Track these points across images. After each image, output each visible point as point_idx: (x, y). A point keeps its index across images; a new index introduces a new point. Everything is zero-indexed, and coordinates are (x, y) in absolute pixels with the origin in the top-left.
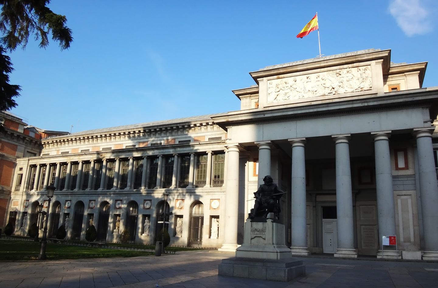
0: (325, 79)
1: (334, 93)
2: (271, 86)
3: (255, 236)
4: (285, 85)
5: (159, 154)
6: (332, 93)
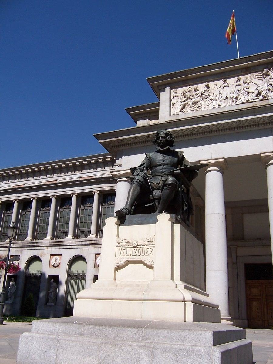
0: (248, 81)
1: (261, 98)
2: (175, 95)
3: (125, 260)
4: (194, 93)
5: (34, 196)
6: (259, 99)
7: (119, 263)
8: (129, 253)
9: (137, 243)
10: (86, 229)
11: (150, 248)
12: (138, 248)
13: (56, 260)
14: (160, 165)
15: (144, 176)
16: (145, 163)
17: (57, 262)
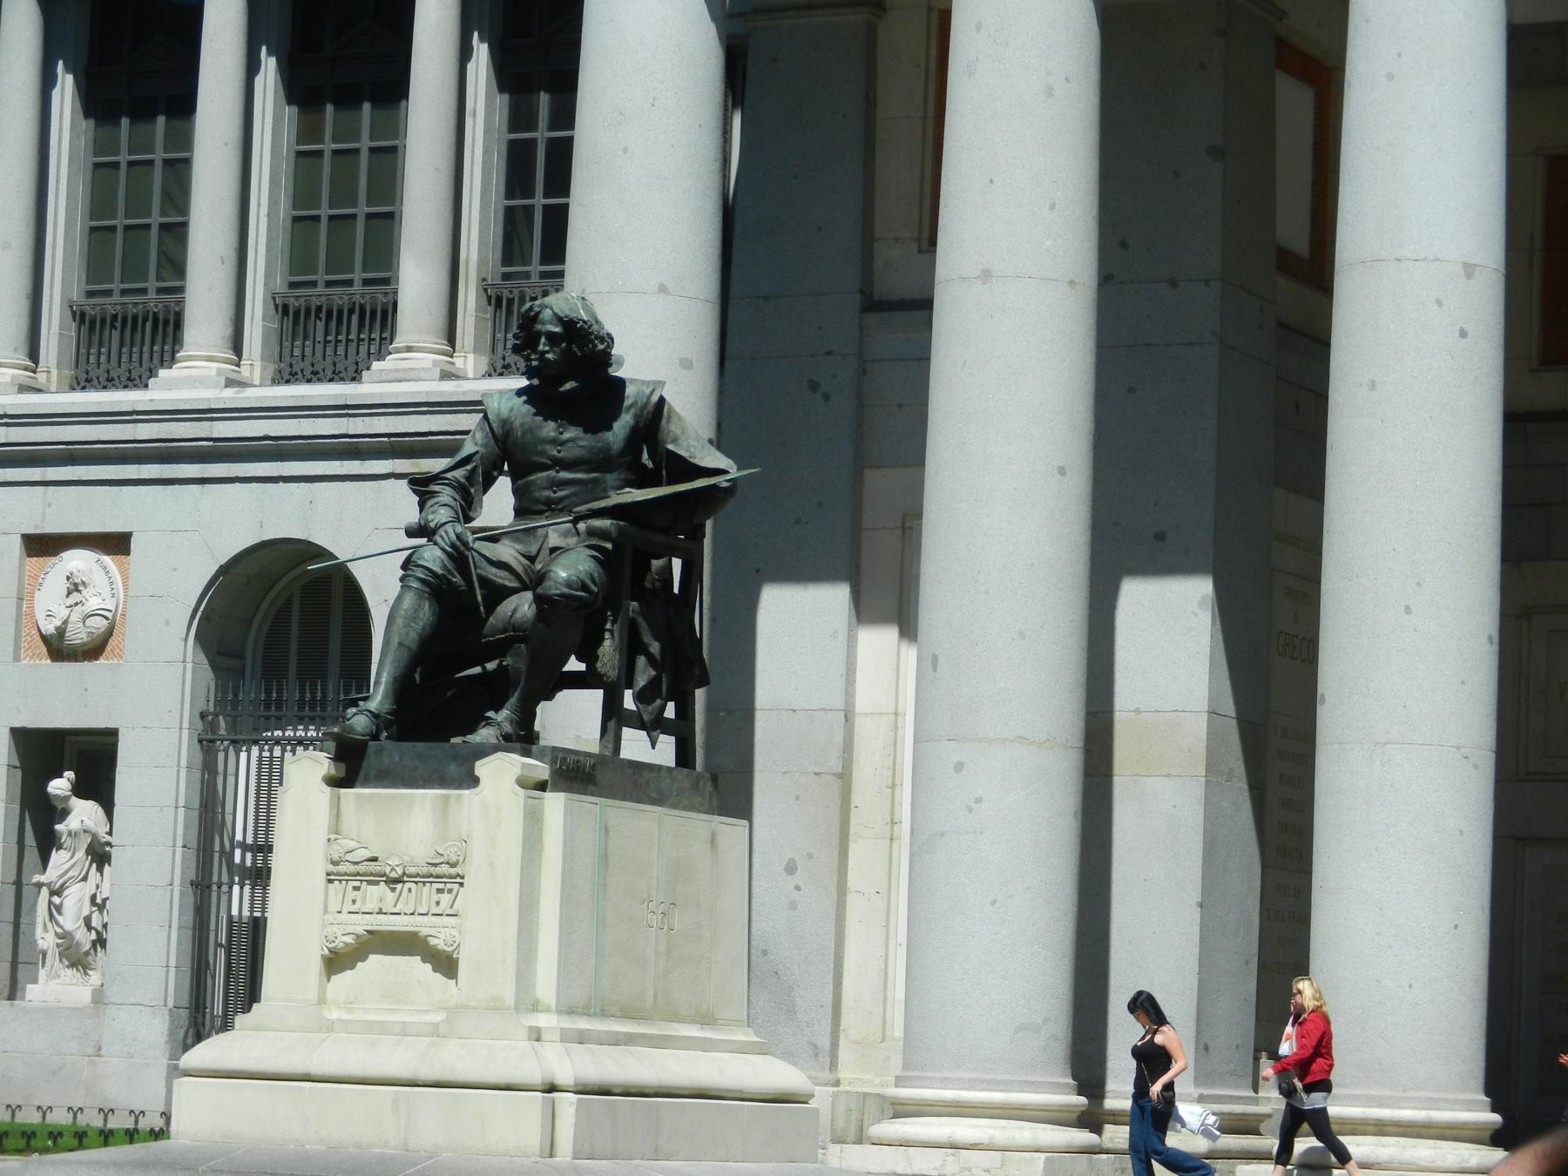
7: (337, 941)
8: (371, 905)
9: (401, 867)
10: (357, 287)
11: (449, 886)
12: (407, 885)
13: (75, 588)
14: (545, 468)
15: (453, 546)
16: (477, 452)
17: (93, 603)
